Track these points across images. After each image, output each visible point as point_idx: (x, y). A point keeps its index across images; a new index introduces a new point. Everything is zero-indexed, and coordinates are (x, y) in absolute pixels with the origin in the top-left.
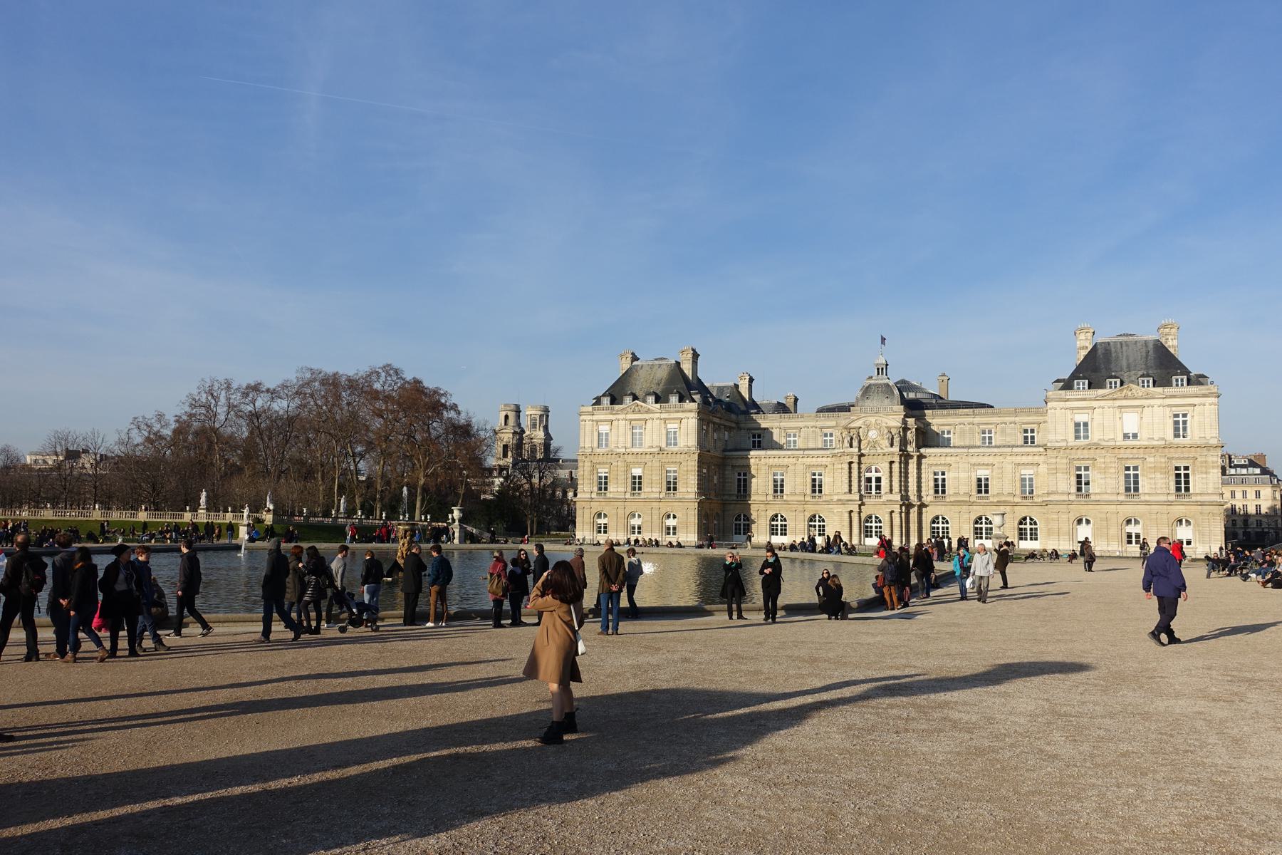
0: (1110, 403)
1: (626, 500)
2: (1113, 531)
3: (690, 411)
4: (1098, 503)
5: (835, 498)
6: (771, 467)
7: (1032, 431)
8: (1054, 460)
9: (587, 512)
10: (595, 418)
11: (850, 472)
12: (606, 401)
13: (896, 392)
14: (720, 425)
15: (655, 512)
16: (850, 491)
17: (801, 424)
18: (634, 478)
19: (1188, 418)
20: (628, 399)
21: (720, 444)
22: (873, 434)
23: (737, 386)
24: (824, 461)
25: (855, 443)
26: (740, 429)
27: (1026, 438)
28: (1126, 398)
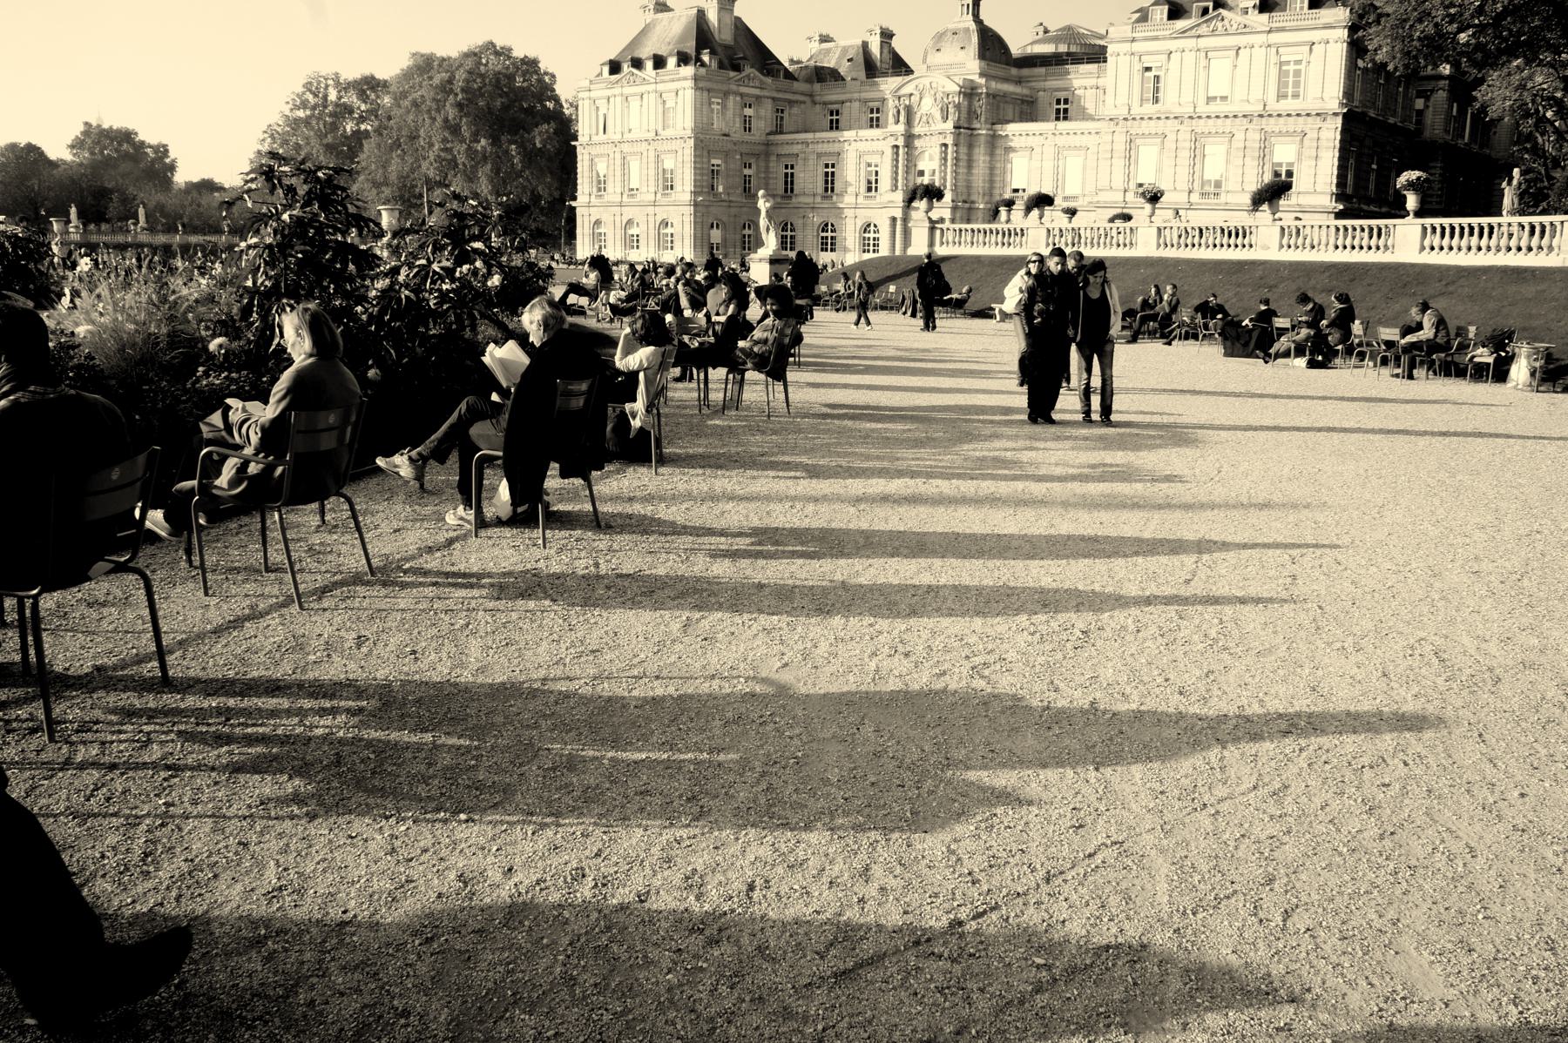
0: (1190, 43)
3: (685, 79)
6: (819, 155)
9: (586, 219)
10: (593, 94)
12: (606, 69)
13: (975, 39)
14: (758, 97)
15: (651, 219)
16: (895, 188)
20: (626, 68)
21: (761, 126)
22: (928, 106)
23: (865, 45)
25: (902, 118)
26: (815, 103)
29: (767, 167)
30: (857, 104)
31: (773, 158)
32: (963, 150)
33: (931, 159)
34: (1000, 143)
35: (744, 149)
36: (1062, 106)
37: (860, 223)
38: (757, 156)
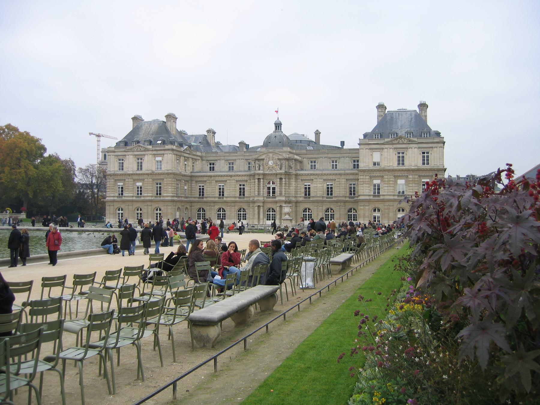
0: (391, 146)
1: (132, 201)
2: (391, 215)
5: (251, 199)
6: (216, 181)
8: (362, 177)
10: (116, 154)
11: (259, 184)
14: (188, 158)
17: (234, 158)
18: (138, 188)
19: (429, 155)
22: (271, 163)
25: (261, 168)
26: (202, 160)
27: (354, 165)
28: (398, 144)
29: (191, 186)
30: (223, 161)
31: (194, 182)
32: (287, 180)
34: (300, 177)
35: (186, 178)
36: (313, 164)
37: (237, 208)
38: (188, 181)
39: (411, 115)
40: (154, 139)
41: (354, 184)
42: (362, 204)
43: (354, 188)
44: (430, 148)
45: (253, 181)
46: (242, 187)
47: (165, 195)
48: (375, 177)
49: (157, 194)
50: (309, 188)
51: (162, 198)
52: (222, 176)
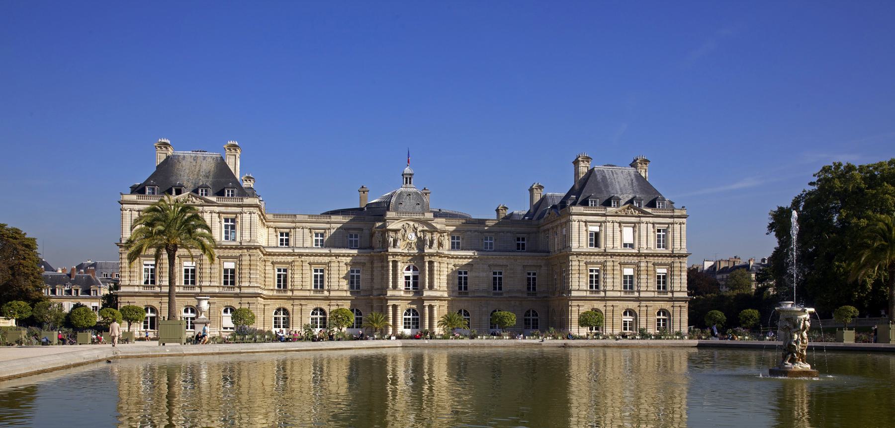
4: (604, 299)
6: (310, 264)
7: (523, 239)
8: (574, 263)
22: (412, 237)
24: (362, 259)
27: (518, 244)
30: (307, 231)
33: (415, 269)
39: (629, 174)
40: (214, 185)
41: (534, 274)
42: (575, 303)
43: (534, 279)
44: (668, 224)
45: (380, 265)
46: (355, 274)
47: (243, 284)
48: (593, 263)
49: (226, 283)
50: (466, 278)
51: (237, 290)
52: (321, 255)
